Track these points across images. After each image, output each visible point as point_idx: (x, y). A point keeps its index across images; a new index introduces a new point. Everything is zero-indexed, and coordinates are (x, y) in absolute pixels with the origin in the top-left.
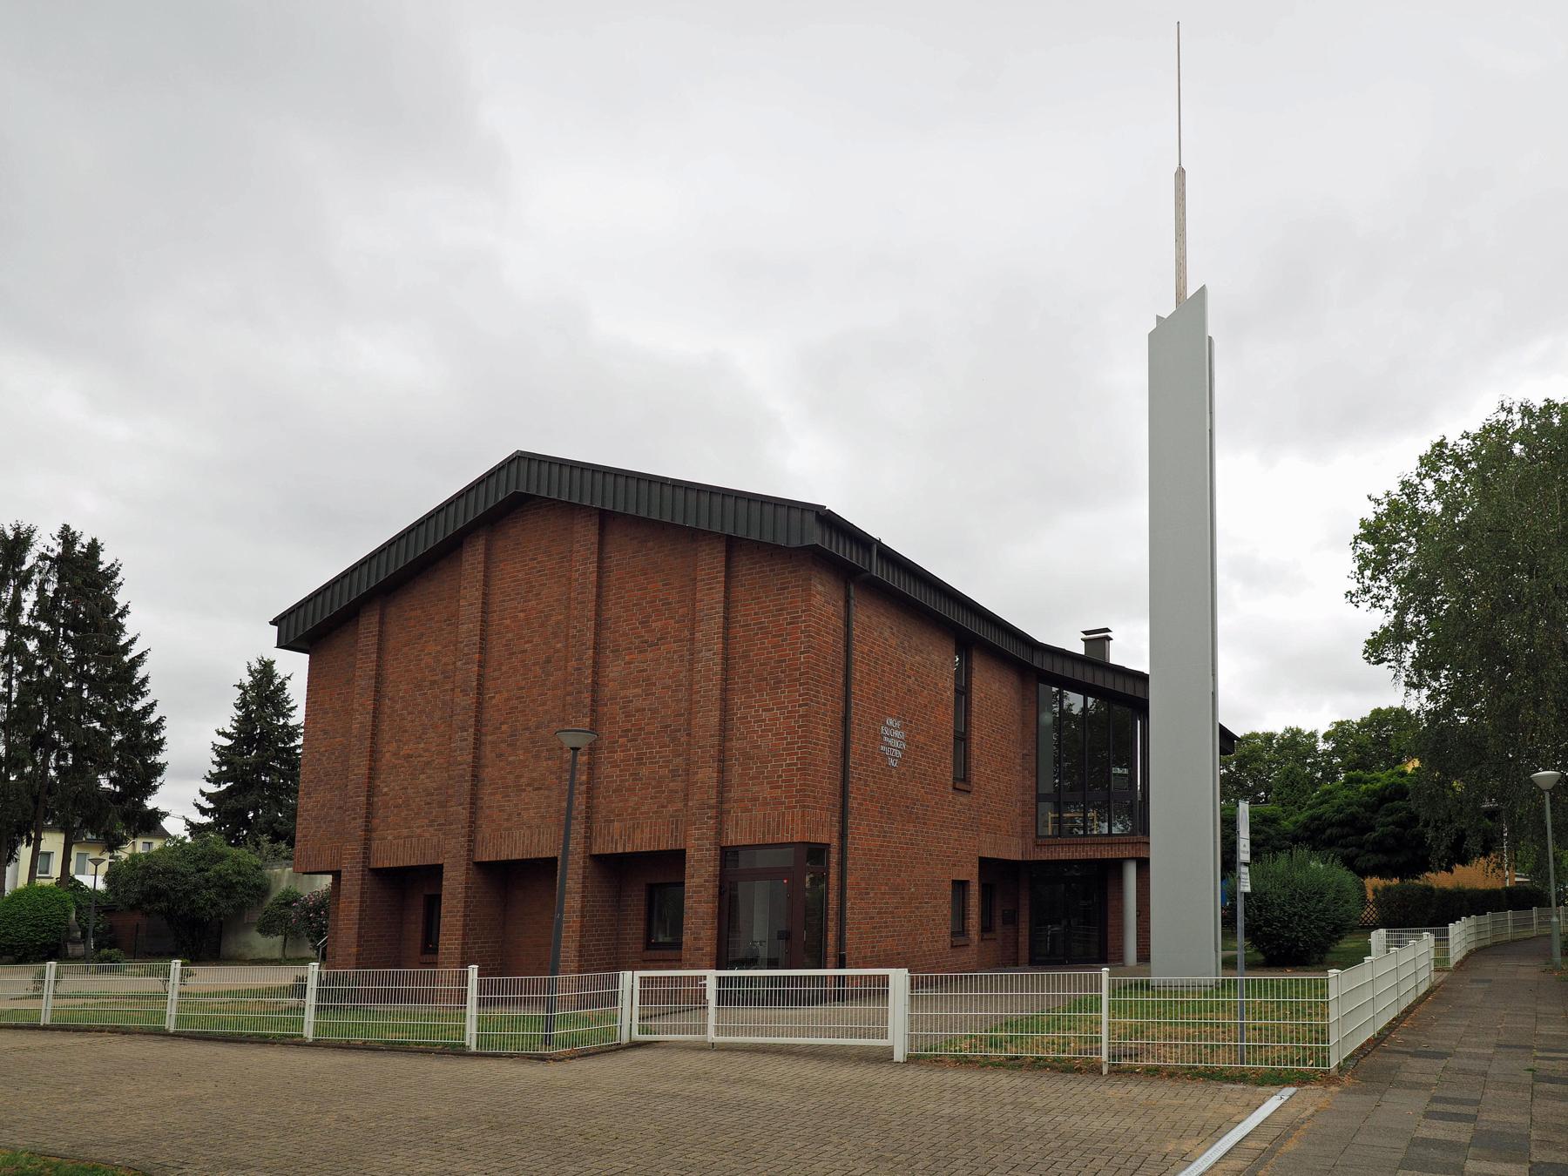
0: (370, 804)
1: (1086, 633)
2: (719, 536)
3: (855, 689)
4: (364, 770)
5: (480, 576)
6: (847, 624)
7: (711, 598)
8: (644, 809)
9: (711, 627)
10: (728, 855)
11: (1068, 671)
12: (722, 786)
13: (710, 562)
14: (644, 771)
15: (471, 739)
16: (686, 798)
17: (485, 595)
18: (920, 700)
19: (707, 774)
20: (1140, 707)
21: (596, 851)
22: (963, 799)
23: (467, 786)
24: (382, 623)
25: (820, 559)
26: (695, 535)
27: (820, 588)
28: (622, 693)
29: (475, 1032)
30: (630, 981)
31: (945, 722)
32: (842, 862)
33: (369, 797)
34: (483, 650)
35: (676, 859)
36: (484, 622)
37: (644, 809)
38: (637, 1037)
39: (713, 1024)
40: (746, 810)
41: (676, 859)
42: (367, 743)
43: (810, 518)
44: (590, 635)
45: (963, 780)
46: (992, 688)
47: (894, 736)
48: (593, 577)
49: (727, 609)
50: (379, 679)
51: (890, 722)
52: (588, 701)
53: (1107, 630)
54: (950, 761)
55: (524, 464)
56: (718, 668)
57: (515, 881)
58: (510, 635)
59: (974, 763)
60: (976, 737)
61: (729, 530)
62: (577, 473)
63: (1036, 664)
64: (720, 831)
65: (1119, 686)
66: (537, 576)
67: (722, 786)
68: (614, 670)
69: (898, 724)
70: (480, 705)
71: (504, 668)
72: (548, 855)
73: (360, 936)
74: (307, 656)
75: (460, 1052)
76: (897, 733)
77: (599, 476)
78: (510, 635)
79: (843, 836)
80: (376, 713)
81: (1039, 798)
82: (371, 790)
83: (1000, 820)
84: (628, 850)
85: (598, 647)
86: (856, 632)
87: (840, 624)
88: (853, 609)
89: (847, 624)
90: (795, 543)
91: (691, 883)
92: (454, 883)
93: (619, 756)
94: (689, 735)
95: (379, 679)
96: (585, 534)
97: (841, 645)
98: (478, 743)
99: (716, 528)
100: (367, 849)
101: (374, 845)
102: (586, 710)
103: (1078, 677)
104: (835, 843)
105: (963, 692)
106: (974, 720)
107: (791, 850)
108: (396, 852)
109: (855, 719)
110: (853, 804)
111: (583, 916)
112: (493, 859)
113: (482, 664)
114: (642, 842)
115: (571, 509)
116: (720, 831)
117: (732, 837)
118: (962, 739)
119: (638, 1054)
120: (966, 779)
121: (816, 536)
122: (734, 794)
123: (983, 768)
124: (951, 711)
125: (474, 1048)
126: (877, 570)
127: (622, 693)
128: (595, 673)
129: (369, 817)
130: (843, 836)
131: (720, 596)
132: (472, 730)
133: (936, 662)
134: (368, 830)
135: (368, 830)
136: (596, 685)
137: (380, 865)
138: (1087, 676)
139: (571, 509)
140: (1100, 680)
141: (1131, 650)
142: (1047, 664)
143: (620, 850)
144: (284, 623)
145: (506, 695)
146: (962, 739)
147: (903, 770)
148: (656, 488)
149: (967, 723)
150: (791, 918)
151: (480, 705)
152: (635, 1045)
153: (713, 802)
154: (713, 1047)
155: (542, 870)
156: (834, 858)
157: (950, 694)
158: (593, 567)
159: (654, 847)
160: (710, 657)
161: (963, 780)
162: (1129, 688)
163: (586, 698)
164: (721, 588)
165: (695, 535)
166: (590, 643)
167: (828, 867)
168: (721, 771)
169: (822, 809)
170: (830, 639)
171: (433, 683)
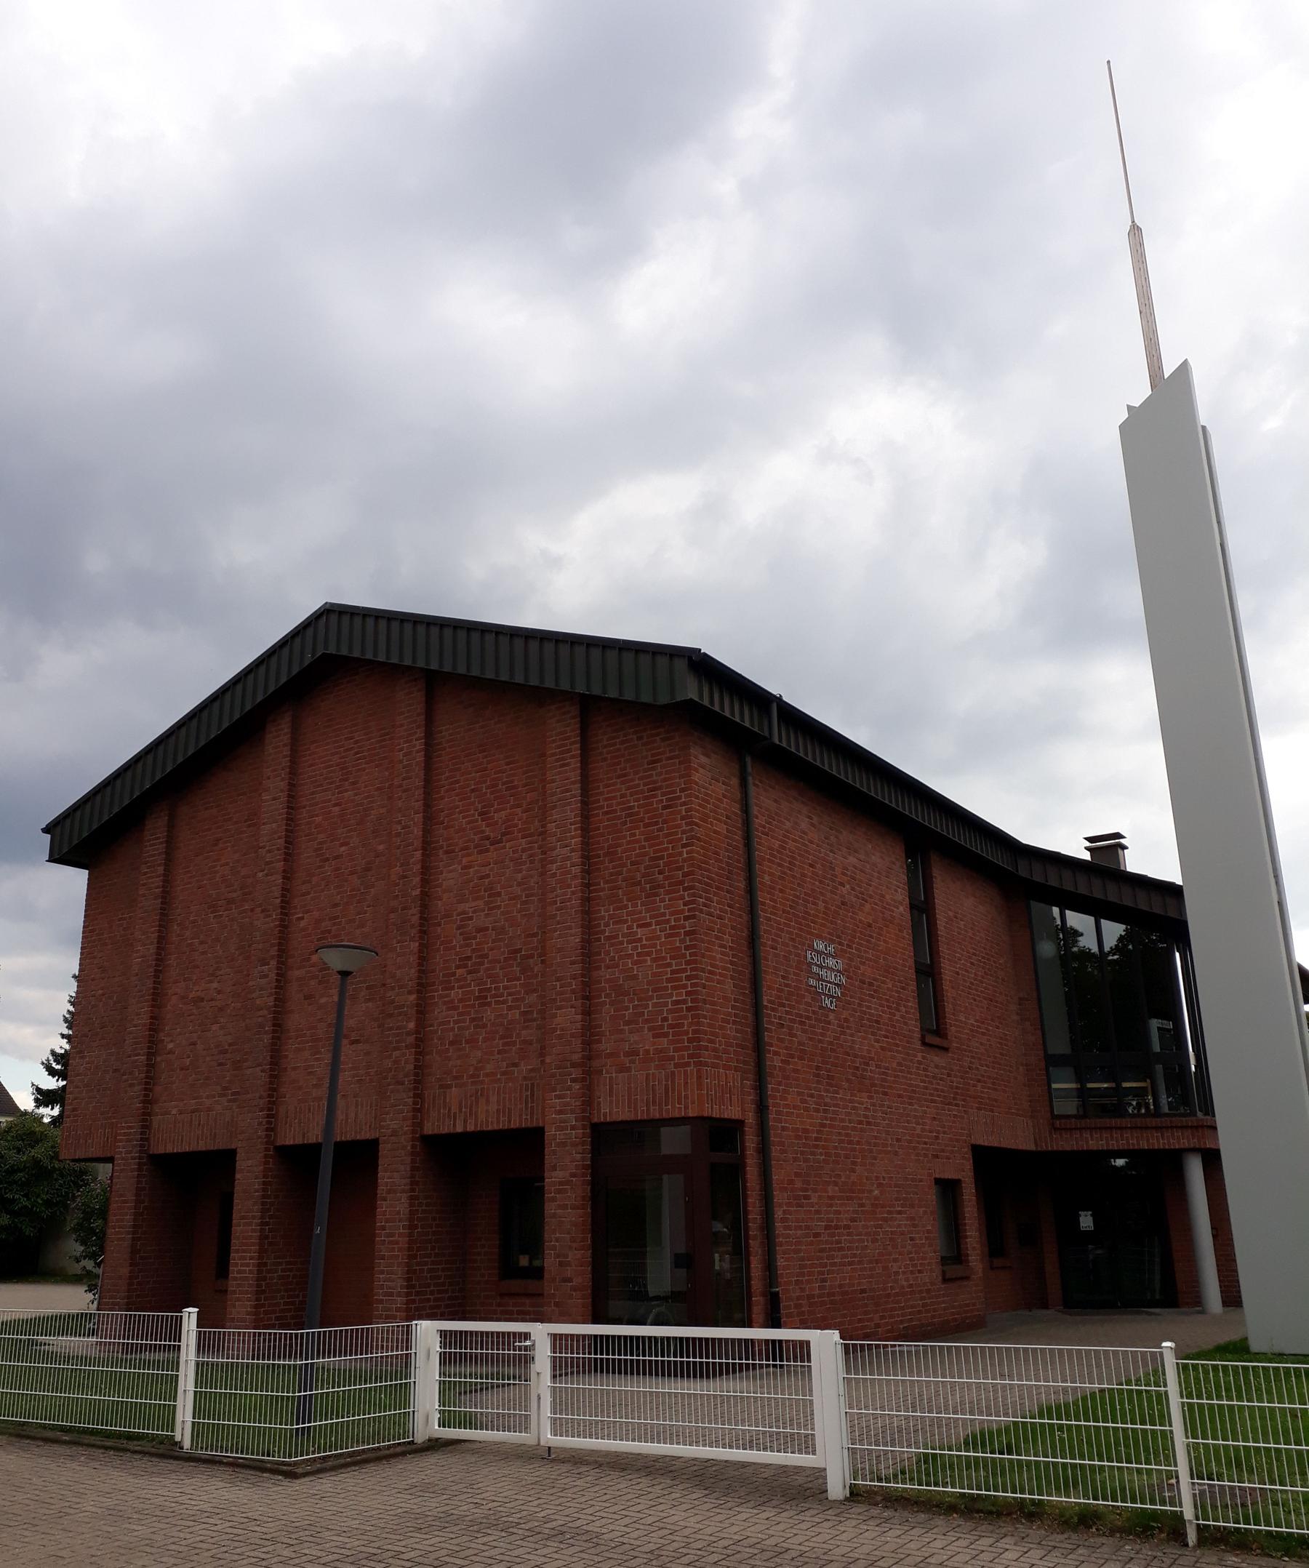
0: (151, 1066)
1: (1089, 839)
2: (568, 696)
3: (762, 896)
4: (145, 1019)
5: (285, 762)
6: (746, 809)
7: (563, 777)
8: (489, 1068)
9: (566, 814)
10: (607, 1139)
11: (1067, 882)
12: (589, 1035)
13: (560, 729)
14: (489, 1014)
15: (273, 976)
16: (542, 1055)
17: (292, 786)
18: (861, 916)
19: (567, 1018)
20: (1178, 933)
21: (429, 1129)
22: (937, 1059)
23: (267, 1039)
24: (171, 826)
25: (695, 719)
26: (538, 696)
27: (703, 759)
28: (461, 907)
29: (189, 1418)
30: (427, 1333)
31: (898, 946)
32: (763, 1150)
33: (150, 1055)
34: (289, 856)
35: (528, 1142)
36: (290, 820)
37: (489, 1068)
38: (437, 1431)
39: (542, 1408)
40: (623, 1069)
41: (528, 1142)
42: (150, 983)
43: (681, 665)
44: (417, 832)
45: (935, 1032)
46: (963, 909)
47: (828, 968)
48: (420, 758)
49: (585, 791)
50: (166, 897)
51: (820, 946)
52: (415, 920)
53: (1118, 836)
54: (913, 1004)
55: (334, 618)
56: (576, 870)
57: (327, 1177)
58: (321, 837)
59: (949, 1008)
60: (947, 972)
61: (581, 689)
62: (395, 625)
63: (1023, 873)
64: (588, 1101)
65: (1142, 902)
66: (355, 760)
67: (589, 1035)
68: (449, 877)
69: (831, 949)
70: (284, 927)
71: (315, 880)
72: (368, 1136)
73: (134, 1251)
74: (84, 874)
75: (167, 1451)
76: (831, 962)
77: (421, 629)
78: (321, 837)
79: (761, 1108)
80: (162, 942)
81: (1052, 1061)
82: (153, 1046)
83: (995, 1091)
84: (471, 1128)
85: (428, 847)
86: (759, 821)
87: (736, 808)
88: (752, 790)
89: (746, 809)
90: (663, 699)
91: (553, 1178)
92: (250, 1175)
93: (456, 994)
94: (543, 962)
95: (166, 897)
96: (408, 704)
97: (738, 837)
98: (281, 980)
99: (565, 685)
100: (146, 1126)
101: (156, 1120)
102: (414, 932)
103: (1082, 890)
104: (750, 1119)
105: (922, 908)
106: (943, 949)
107: (686, 1129)
108: (181, 1133)
109: (766, 939)
110: (774, 1061)
111: (412, 1227)
112: (299, 1141)
113: (288, 875)
114: (489, 1116)
115: (389, 672)
116: (588, 1101)
117: (605, 1109)
118: (928, 972)
119: (432, 1459)
120: (940, 1032)
121: (691, 690)
122: (606, 1046)
123: (963, 1016)
124: (907, 934)
125: (187, 1444)
126: (779, 736)
127: (461, 907)
128: (425, 882)
129: (149, 1083)
130: (761, 1108)
131: (575, 776)
132: (273, 963)
133: (877, 868)
134: (148, 1101)
135: (148, 1101)
136: (425, 899)
137: (161, 1150)
138: (1097, 890)
139: (389, 672)
140: (1113, 894)
141: (1154, 855)
142: (1038, 874)
143: (459, 1129)
144: (58, 829)
145: (316, 914)
146: (928, 972)
147: (845, 1014)
148: (490, 638)
149: (934, 952)
150: (671, 1236)
151: (284, 927)
152: (435, 1445)
153: (576, 1057)
154: (549, 1456)
155: (359, 1159)
156: (751, 1141)
157: (902, 911)
158: (419, 745)
159: (502, 1125)
160: (566, 852)
161: (935, 1032)
162: (1156, 905)
163: (414, 915)
164: (575, 763)
165: (538, 696)
166: (418, 843)
167: (743, 1156)
168: (587, 1013)
169: (726, 1067)
170: (722, 828)
171: (230, 901)
